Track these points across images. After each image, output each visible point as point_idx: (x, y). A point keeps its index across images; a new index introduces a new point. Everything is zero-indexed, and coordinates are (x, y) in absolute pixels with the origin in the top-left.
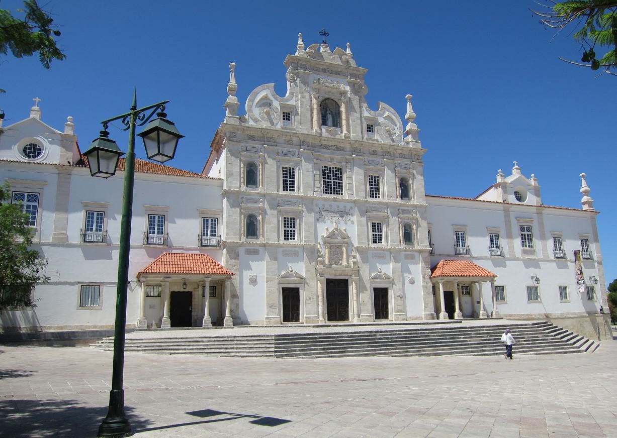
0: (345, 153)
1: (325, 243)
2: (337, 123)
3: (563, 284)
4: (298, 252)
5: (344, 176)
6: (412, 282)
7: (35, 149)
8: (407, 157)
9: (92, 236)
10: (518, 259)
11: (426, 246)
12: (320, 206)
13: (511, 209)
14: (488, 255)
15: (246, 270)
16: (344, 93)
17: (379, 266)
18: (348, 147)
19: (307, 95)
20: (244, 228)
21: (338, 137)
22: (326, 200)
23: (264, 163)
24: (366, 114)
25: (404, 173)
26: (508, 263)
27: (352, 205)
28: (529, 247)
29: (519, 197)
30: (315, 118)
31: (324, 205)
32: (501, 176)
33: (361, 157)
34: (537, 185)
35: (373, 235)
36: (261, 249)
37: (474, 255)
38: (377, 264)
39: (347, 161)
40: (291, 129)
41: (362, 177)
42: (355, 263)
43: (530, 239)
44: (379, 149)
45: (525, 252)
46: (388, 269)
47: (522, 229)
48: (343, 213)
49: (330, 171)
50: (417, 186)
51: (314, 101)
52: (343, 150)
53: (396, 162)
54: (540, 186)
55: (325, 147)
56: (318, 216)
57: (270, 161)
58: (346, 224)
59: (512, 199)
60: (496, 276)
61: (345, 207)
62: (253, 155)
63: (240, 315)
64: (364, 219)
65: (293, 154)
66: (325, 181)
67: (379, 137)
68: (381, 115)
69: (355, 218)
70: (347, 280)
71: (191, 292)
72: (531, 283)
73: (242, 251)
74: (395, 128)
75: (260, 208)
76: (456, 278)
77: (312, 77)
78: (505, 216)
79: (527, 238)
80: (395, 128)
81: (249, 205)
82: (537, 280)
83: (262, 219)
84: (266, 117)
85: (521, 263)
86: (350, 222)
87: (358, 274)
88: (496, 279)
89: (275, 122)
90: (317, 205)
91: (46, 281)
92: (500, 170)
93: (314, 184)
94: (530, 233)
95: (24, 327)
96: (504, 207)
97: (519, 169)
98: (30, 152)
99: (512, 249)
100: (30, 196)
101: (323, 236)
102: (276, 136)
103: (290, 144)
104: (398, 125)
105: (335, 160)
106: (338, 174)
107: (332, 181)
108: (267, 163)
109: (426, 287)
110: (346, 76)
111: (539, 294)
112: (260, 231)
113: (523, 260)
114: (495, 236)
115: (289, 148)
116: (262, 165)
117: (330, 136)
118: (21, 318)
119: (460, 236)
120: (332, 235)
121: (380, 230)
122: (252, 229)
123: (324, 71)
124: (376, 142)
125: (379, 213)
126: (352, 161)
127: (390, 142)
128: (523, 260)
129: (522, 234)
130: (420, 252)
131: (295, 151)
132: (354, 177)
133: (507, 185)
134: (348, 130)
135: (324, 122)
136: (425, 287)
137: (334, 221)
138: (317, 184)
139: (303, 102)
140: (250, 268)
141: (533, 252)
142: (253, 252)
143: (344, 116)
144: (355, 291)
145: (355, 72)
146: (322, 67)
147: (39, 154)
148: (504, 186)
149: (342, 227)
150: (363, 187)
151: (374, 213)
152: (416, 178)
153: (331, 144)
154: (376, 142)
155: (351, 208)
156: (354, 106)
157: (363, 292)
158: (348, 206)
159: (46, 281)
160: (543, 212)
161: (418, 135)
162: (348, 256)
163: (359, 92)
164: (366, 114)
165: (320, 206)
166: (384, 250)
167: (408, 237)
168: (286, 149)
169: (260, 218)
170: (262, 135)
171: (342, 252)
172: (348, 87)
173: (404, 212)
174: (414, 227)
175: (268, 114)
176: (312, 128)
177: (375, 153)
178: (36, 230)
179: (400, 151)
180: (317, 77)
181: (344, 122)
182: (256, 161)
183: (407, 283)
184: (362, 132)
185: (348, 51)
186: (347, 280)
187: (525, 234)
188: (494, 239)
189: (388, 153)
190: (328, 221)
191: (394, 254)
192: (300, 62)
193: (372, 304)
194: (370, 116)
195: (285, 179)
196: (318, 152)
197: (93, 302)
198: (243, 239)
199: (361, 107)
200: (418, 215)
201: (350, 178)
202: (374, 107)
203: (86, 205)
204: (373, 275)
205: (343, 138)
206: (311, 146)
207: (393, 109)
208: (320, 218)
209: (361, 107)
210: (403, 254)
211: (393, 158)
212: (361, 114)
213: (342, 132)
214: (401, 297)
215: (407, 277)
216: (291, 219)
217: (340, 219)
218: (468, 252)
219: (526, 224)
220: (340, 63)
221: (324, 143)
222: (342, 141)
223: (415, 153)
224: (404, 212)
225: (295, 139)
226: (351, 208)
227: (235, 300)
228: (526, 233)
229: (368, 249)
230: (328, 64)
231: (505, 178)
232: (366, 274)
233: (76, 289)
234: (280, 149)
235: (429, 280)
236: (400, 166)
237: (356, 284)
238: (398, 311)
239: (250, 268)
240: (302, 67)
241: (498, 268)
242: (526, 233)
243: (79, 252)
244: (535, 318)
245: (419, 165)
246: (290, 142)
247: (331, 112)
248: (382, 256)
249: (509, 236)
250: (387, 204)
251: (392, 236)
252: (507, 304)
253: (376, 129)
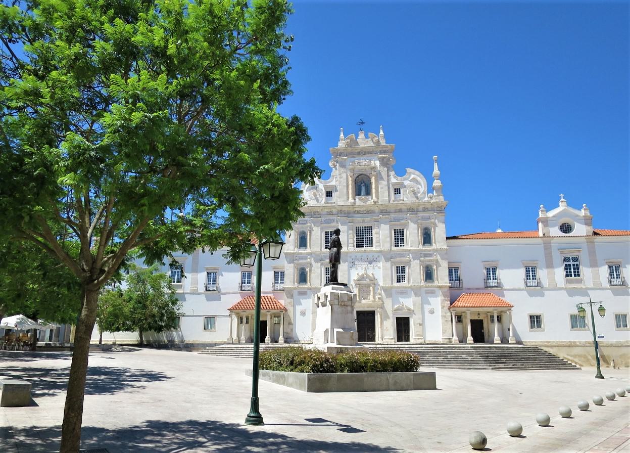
0: (374, 214)
1: (356, 285)
2: (368, 193)
5: (374, 231)
6: (432, 312)
8: (430, 209)
9: (211, 287)
10: (560, 289)
11: (446, 283)
12: (353, 257)
13: (552, 241)
14: (523, 286)
15: (298, 305)
16: (374, 168)
17: (401, 300)
18: (377, 209)
19: (344, 175)
20: (297, 278)
21: (368, 203)
22: (358, 252)
23: (311, 230)
24: (393, 180)
25: (426, 223)
26: (546, 292)
27: (379, 254)
28: (575, 276)
29: (566, 228)
30: (350, 191)
31: (356, 256)
32: (542, 211)
33: (387, 216)
34: (589, 214)
35: (398, 276)
36: (309, 291)
37: (506, 287)
38: (400, 299)
39: (376, 221)
40: (332, 203)
41: (387, 232)
42: (379, 298)
43: (577, 267)
44: (404, 208)
45: (567, 282)
46: (409, 303)
47: (567, 259)
48: (371, 262)
50: (439, 233)
51: (350, 179)
52: (373, 212)
53: (419, 215)
54: (592, 216)
55: (358, 212)
56: (351, 264)
57: (315, 228)
59: (555, 231)
62: (303, 226)
63: (294, 336)
64: (389, 264)
65: (332, 221)
67: (406, 198)
68: (405, 179)
69: (380, 264)
70: (374, 311)
72: (575, 312)
73: (295, 293)
74: (420, 187)
75: (307, 263)
76: (496, 308)
77: (348, 160)
78: (545, 249)
79: (572, 268)
80: (420, 187)
81: (301, 261)
83: (310, 270)
84: (314, 197)
85: (564, 292)
86: (377, 267)
87: (382, 307)
88: (512, 309)
89: (320, 199)
91: (183, 315)
92: (541, 206)
93: (348, 241)
95: (177, 340)
96: (543, 240)
97: (565, 202)
99: (552, 278)
101: (355, 280)
102: (319, 210)
103: (330, 214)
104: (423, 185)
105: (366, 221)
106: (369, 230)
107: (364, 237)
108: (313, 231)
109: (445, 317)
110: (376, 153)
111: (586, 322)
112: (308, 278)
113: (565, 289)
115: (331, 217)
116: (310, 233)
117: (362, 204)
118: (175, 335)
119: (491, 271)
120: (361, 278)
121: (404, 272)
122: (303, 277)
123: (359, 153)
124: (401, 202)
125: (402, 259)
126: (380, 220)
127: (414, 200)
128: (565, 289)
129: (566, 265)
130: (440, 287)
132: (381, 232)
133: (549, 219)
134: (377, 197)
135: (358, 193)
136: (444, 317)
137: (364, 268)
138: (351, 241)
139: (341, 181)
140: (300, 304)
141: (581, 281)
142: (303, 293)
143: (373, 186)
144: (379, 320)
145: (384, 149)
146: (357, 151)
148: (546, 222)
149: (370, 273)
150: (388, 239)
151: (398, 259)
152: (437, 227)
153: (362, 209)
154: (401, 202)
155: (379, 256)
156: (383, 176)
157: (386, 320)
158: (376, 255)
159: (183, 315)
160: (595, 240)
161: (442, 190)
162: (374, 293)
163: (387, 164)
164: (393, 180)
165: (353, 257)
166: (406, 288)
167: (429, 275)
168: (327, 218)
169: (308, 270)
170: (309, 211)
171: (370, 291)
172: (378, 162)
173: (426, 255)
174: (435, 267)
175: (315, 195)
176: (348, 200)
177: (400, 211)
178: (182, 285)
179: (423, 206)
180: (353, 159)
181: (374, 191)
182: (304, 230)
183: (427, 314)
184: (389, 195)
185: (381, 132)
186: (374, 311)
187: (570, 265)
188: (531, 272)
189: (412, 210)
190: (359, 268)
191: (417, 291)
192: (339, 152)
193: (395, 330)
194: (397, 181)
196: (352, 217)
197: (211, 328)
198: (296, 285)
199: (388, 176)
200: (439, 257)
201: (378, 233)
202: (401, 173)
203: (207, 269)
204: (396, 307)
205: (373, 203)
206: (346, 213)
207: (418, 172)
208: (353, 265)
209: (388, 176)
210: (423, 290)
211: (416, 213)
212: (388, 181)
213: (372, 199)
214: (420, 325)
215: (427, 308)
217: (369, 265)
218: (499, 285)
220: (372, 144)
221: (357, 209)
222: (371, 206)
223: (436, 206)
224: (426, 255)
225: (334, 210)
226: (379, 256)
227: (291, 326)
228: (571, 263)
229: (392, 287)
230: (361, 148)
231: (547, 212)
232: (389, 306)
233: (202, 320)
234: (323, 219)
235: (448, 311)
236: (423, 218)
237: (381, 315)
238: (418, 336)
239: (300, 304)
240: (340, 155)
241: (534, 297)
243: (203, 297)
244: (580, 345)
245: (442, 215)
246: (331, 213)
247: (365, 184)
248: (404, 292)
249: (550, 265)
250: (409, 251)
251: (415, 274)
252: (544, 331)
253: (402, 191)
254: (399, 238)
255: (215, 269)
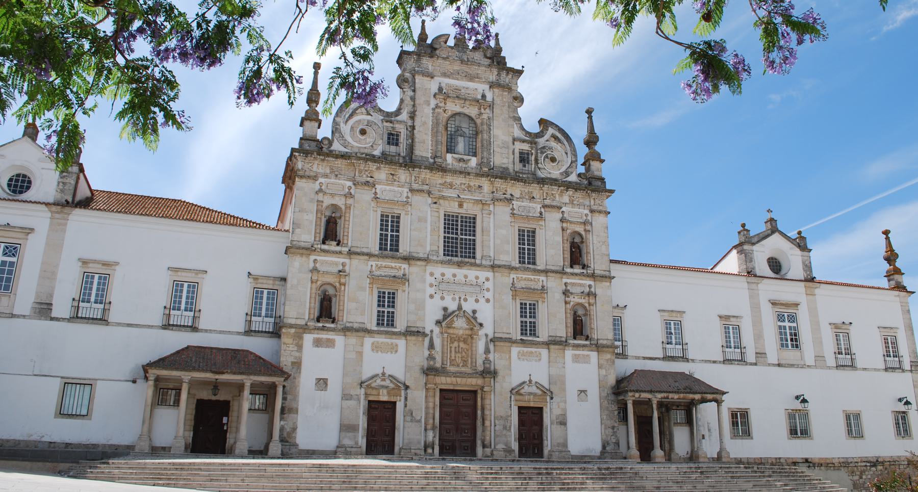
3: (853, 408)
4: (397, 345)
7: (23, 181)
49: (457, 221)
58: (477, 301)
60: (724, 393)
61: (477, 278)
66: (448, 238)
71: (198, 401)
82: (804, 401)
88: (724, 397)
90: (432, 274)
94: (795, 325)
98: (16, 186)
100: (7, 248)
114: (733, 328)
121: (533, 315)
129: (780, 327)
131: (403, 191)
147: (28, 188)
149: (468, 307)
187: (785, 327)
195: (384, 233)
216: (389, 293)
219: (786, 311)
228: (787, 324)
242: (787, 324)
254: (526, 247)
255: (106, 264)
